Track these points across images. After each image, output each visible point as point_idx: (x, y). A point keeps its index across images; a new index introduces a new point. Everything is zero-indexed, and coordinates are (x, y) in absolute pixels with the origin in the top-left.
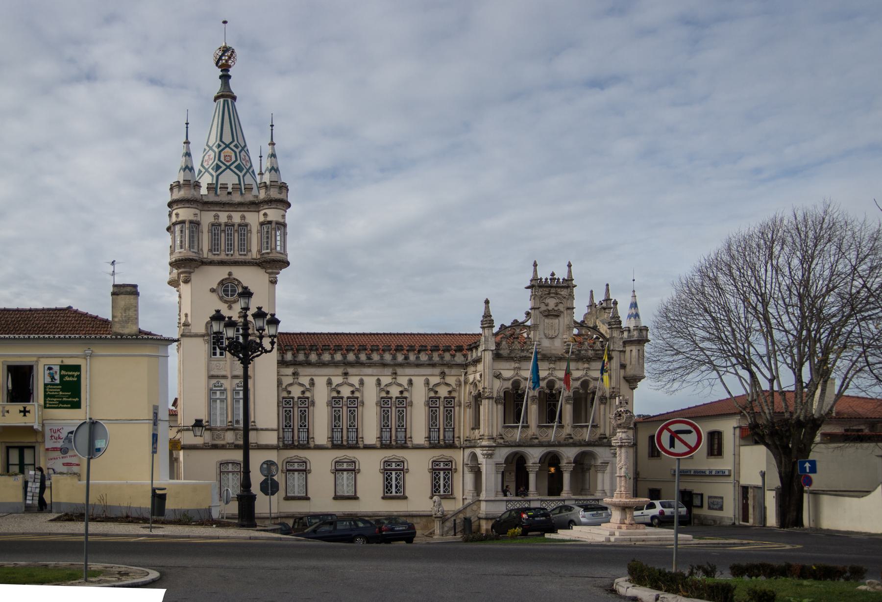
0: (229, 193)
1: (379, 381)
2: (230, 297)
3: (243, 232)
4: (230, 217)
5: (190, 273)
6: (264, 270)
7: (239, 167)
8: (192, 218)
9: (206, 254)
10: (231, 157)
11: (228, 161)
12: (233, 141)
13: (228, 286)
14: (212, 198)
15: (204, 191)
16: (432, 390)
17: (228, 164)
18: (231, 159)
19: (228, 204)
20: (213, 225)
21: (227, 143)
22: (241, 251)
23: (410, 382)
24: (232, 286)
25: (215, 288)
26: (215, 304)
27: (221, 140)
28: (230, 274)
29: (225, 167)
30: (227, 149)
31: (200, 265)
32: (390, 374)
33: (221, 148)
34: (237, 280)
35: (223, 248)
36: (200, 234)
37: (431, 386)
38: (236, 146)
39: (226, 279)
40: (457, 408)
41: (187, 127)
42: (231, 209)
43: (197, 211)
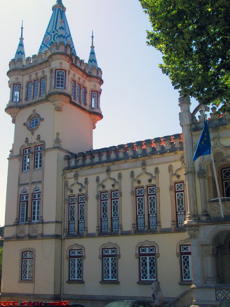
2: (34, 127)
3: (43, 82)
4: (36, 74)
5: (15, 117)
6: (52, 103)
9: (24, 102)
10: (48, 39)
11: (46, 42)
12: (53, 29)
13: (33, 120)
14: (28, 66)
15: (25, 63)
17: (46, 44)
19: (34, 66)
22: (42, 95)
23: (157, 170)
24: (36, 119)
25: (26, 122)
26: (27, 133)
28: (34, 111)
29: (44, 46)
30: (49, 35)
31: (20, 110)
33: (45, 36)
36: (21, 90)
37: (174, 172)
38: (54, 32)
39: (32, 115)
41: (22, 30)
43: (19, 76)
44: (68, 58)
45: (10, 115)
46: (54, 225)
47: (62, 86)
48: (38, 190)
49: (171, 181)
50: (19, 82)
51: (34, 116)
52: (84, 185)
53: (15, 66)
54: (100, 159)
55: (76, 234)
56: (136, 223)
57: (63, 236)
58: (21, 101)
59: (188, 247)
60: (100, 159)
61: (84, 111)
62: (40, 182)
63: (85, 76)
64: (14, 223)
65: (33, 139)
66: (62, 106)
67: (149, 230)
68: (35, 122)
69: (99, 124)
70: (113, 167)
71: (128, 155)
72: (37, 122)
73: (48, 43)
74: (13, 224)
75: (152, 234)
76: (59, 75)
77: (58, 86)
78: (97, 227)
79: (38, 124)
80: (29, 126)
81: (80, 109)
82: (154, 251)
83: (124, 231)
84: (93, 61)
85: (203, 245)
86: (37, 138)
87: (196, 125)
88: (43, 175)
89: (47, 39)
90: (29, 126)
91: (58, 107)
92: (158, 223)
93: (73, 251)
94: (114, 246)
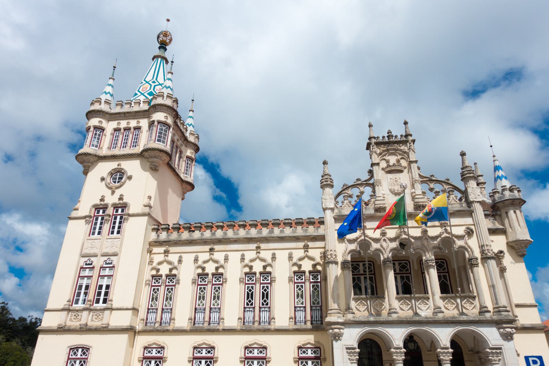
0: (132, 107)
1: (243, 255)
4: (128, 123)
7: (150, 94)
8: (97, 124)
9: (105, 151)
10: (146, 88)
13: (117, 175)
16: (295, 264)
17: (143, 92)
18: (146, 90)
20: (116, 130)
21: (148, 81)
23: (274, 258)
25: (105, 176)
27: (145, 80)
30: (147, 84)
31: (98, 160)
32: (255, 248)
34: (123, 169)
35: (119, 145)
36: (104, 137)
37: (295, 260)
38: (154, 82)
39: (115, 169)
40: (323, 283)
42: (130, 118)
43: (103, 121)
44: (175, 113)
45: (81, 163)
46: (131, 312)
47: (163, 142)
48: (111, 263)
49: (290, 270)
50: (102, 127)
51: (118, 171)
52: (176, 263)
53: (100, 106)
54: (202, 234)
55: (158, 327)
56: (242, 317)
57: (137, 327)
58: (101, 149)
59: (307, 351)
60: (202, 234)
61: (177, 177)
62: (115, 255)
63: (183, 140)
64: (65, 305)
65: (111, 199)
66: (159, 165)
67: (260, 326)
68: (119, 177)
69: (188, 195)
70: (217, 247)
71: (239, 234)
72: (121, 178)
73: (145, 92)
74: (61, 307)
75: (317, 331)
76: (162, 130)
77: (159, 141)
78: (189, 319)
79: (123, 181)
80: (110, 182)
81: (174, 175)
82: (264, 354)
83: (227, 327)
84: (191, 126)
85: (347, 348)
86: (119, 197)
87: (339, 211)
88: (121, 244)
89: (144, 88)
90: (109, 181)
91: (155, 165)
92: (271, 319)
93: (150, 350)
94: (212, 345)
